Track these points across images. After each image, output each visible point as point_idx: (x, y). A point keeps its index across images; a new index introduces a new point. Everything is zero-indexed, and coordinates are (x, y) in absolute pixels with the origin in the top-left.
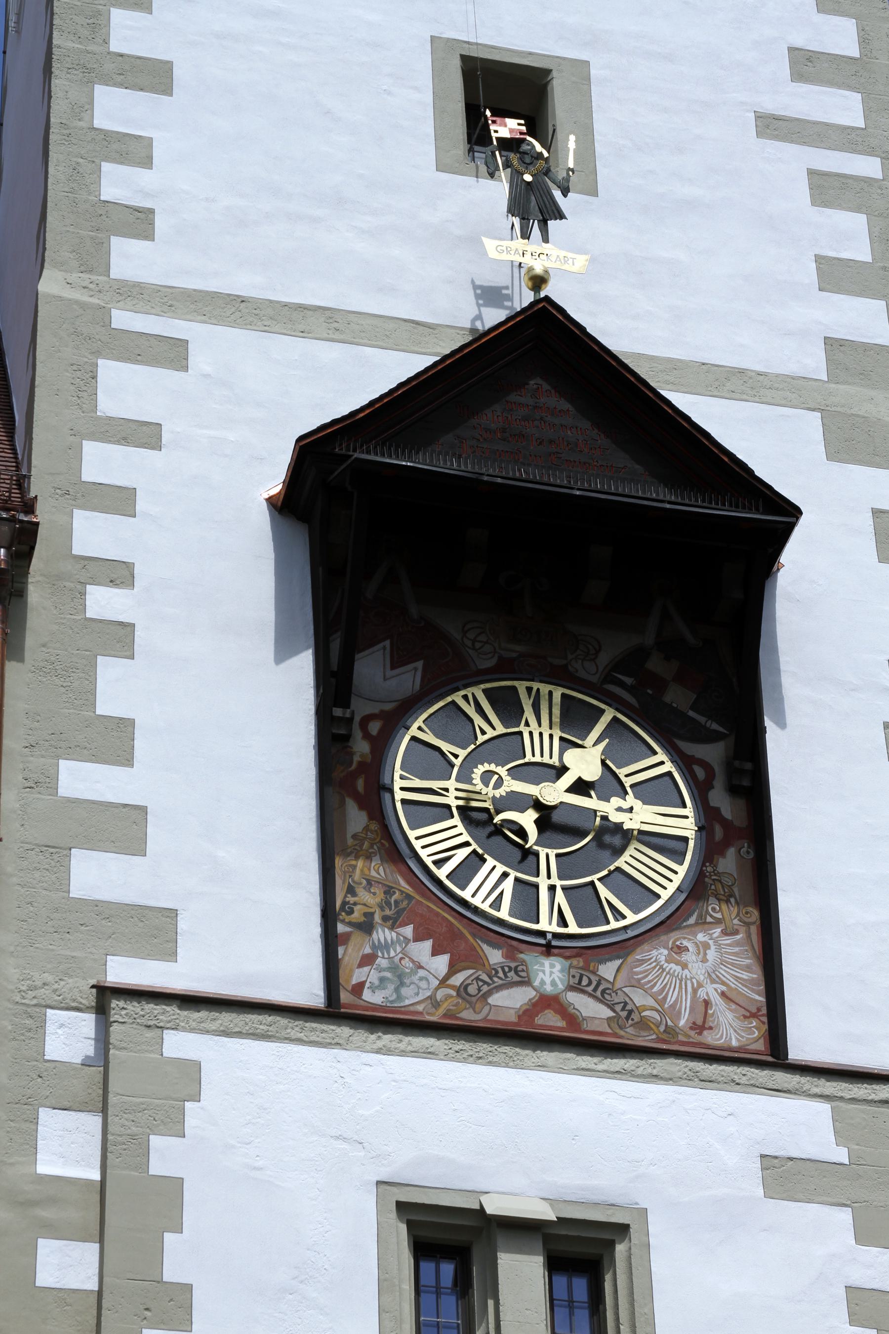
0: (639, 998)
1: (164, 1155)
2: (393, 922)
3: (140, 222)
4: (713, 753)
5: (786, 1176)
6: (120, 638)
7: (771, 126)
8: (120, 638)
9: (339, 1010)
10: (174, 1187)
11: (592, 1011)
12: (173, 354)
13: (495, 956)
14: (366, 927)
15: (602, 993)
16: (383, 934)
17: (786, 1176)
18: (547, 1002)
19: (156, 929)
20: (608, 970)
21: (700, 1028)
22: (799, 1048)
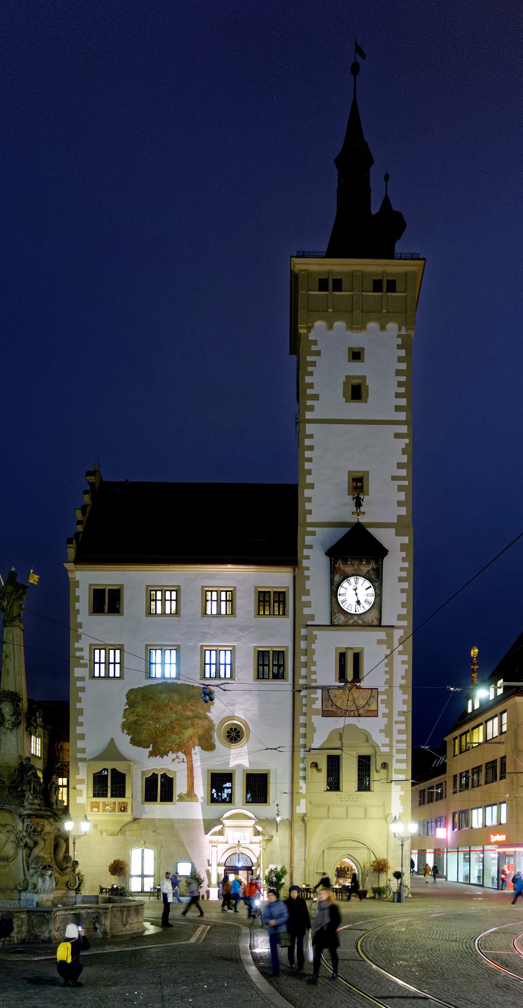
0: (365, 619)
1: (313, 646)
2: (338, 613)
3: (310, 512)
4: (376, 584)
5: (380, 642)
6: (308, 578)
7: (394, 478)
8: (308, 578)
9: (332, 625)
10: (314, 650)
11: (360, 622)
12: (313, 533)
13: (350, 616)
14: (335, 614)
15: (361, 620)
16: (337, 615)
17: (380, 642)
18: (355, 621)
19: (312, 617)
20: (362, 616)
21: (372, 623)
22: (382, 624)
